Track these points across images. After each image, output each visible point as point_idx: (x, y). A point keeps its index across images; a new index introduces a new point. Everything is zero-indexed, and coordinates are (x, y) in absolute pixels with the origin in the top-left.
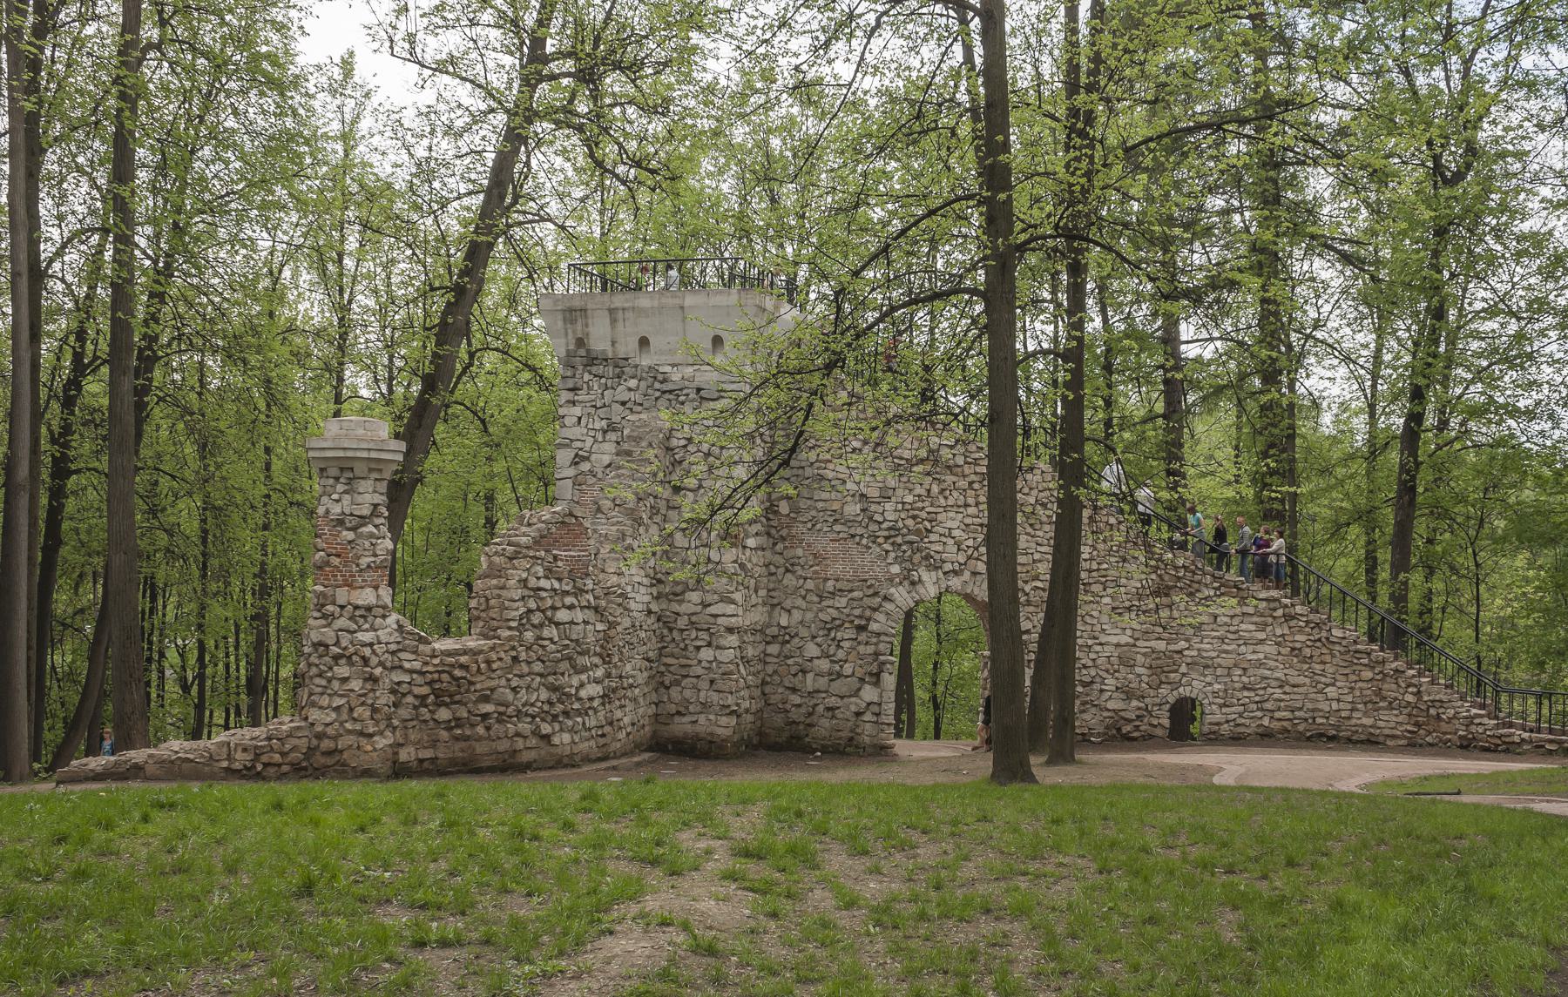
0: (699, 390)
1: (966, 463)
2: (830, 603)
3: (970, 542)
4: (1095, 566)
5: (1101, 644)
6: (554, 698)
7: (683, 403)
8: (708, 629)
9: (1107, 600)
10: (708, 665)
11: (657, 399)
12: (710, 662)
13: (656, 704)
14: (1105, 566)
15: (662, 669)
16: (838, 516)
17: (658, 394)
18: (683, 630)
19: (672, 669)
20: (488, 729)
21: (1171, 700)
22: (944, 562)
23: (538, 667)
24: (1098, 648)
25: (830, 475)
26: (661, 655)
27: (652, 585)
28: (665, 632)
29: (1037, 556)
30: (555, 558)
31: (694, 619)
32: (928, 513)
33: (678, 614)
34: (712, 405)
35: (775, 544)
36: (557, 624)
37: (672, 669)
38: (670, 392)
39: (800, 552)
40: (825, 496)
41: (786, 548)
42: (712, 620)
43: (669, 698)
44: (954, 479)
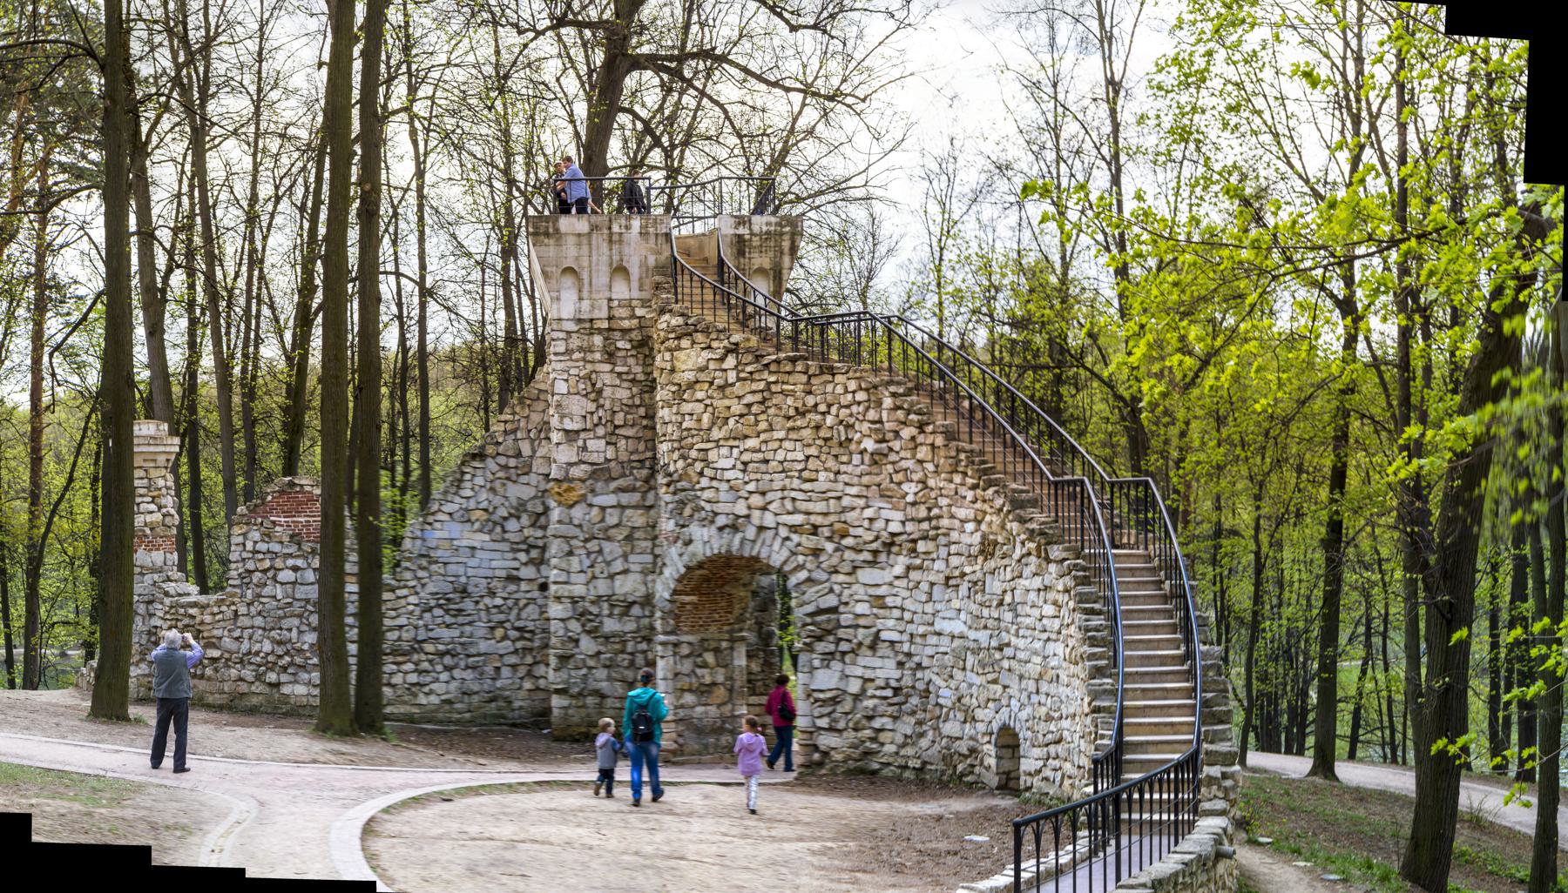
1: (739, 379)
3: (751, 487)
4: (923, 513)
5: (939, 634)
9: (940, 565)
14: (935, 511)
20: (216, 670)
21: (995, 726)
22: (716, 514)
23: (259, 621)
24: (933, 640)
29: (846, 501)
30: (274, 523)
32: (700, 450)
44: (727, 402)
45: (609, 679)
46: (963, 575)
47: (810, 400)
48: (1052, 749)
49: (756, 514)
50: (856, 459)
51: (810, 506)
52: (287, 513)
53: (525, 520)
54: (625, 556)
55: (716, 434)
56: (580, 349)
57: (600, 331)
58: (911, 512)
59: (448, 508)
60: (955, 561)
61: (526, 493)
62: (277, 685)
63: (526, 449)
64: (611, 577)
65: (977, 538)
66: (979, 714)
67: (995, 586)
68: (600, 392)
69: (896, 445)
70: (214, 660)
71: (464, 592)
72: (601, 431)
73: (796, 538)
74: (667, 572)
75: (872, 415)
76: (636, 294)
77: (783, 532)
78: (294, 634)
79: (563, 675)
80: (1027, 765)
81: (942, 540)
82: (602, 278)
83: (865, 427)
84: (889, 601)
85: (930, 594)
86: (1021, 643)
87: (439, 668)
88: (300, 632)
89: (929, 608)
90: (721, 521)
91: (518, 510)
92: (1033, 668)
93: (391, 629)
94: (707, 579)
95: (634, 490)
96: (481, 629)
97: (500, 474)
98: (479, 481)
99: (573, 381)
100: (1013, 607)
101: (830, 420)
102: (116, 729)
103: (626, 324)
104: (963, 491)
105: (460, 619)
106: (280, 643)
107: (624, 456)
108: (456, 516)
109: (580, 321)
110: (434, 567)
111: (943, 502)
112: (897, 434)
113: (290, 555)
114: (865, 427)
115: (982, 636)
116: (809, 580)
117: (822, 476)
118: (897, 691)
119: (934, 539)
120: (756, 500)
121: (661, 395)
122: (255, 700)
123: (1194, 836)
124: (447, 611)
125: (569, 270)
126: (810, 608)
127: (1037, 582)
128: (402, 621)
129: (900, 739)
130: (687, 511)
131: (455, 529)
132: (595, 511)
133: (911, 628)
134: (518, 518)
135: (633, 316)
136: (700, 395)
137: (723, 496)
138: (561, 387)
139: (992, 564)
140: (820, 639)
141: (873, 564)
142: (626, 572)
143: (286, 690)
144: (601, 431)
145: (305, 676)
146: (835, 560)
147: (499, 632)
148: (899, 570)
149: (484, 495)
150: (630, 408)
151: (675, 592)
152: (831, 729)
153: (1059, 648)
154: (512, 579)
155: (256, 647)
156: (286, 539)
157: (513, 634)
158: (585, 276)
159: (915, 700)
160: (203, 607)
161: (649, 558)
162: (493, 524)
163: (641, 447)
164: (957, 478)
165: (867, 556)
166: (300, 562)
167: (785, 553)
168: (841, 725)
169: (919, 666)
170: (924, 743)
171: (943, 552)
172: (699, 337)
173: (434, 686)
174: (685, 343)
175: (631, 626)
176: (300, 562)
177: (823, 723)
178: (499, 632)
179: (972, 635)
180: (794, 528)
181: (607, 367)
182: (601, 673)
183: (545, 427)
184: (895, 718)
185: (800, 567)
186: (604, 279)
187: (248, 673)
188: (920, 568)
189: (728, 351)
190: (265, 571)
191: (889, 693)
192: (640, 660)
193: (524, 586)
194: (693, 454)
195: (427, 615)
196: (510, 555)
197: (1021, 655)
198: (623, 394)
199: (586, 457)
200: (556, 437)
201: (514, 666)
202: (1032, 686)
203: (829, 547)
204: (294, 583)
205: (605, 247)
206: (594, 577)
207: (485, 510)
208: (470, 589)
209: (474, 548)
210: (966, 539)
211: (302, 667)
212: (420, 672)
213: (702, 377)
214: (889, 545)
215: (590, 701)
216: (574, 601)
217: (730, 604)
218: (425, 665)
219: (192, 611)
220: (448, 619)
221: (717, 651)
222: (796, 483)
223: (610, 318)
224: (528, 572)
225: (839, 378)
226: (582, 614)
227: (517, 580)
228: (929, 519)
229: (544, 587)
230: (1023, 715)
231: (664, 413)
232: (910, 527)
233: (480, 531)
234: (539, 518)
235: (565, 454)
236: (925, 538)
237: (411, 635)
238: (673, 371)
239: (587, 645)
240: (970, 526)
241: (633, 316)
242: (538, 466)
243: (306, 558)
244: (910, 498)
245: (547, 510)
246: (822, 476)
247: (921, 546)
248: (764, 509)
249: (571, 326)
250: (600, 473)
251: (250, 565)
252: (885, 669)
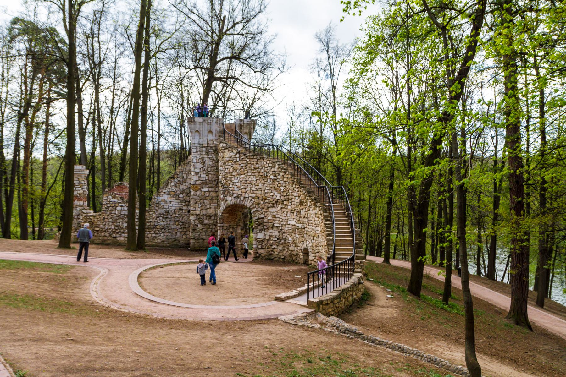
3: (243, 187)
4: (285, 194)
6: (116, 228)
21: (303, 248)
23: (111, 220)
24: (287, 226)
27: (181, 202)
29: (266, 191)
45: (206, 235)
46: (295, 210)
47: (258, 166)
48: (317, 254)
49: (244, 194)
50: (269, 180)
51: (257, 192)
52: (120, 191)
53: (184, 194)
54: (210, 204)
55: (234, 174)
56: (200, 151)
57: (205, 147)
58: (282, 194)
59: (164, 191)
60: (293, 206)
61: (185, 187)
62: (115, 237)
63: (185, 176)
64: (207, 209)
65: (299, 201)
66: (299, 245)
67: (303, 213)
68: (204, 162)
69: (279, 177)
70: (97, 231)
71: (168, 213)
72: (204, 172)
73: (253, 200)
74: (221, 208)
75: (273, 169)
76: (214, 138)
77: (250, 198)
78: (121, 224)
79: (194, 234)
80: (310, 258)
81: (290, 201)
82: (206, 132)
83: (271, 173)
84: (277, 216)
85: (287, 215)
86: (309, 227)
88: (123, 223)
89: (286, 218)
90: (235, 195)
91: (183, 192)
92: (312, 234)
93: (148, 222)
94: (231, 210)
95: (213, 187)
96: (172, 222)
98: (173, 184)
99: (198, 159)
100: (307, 218)
101: (262, 171)
102: (66, 251)
103: (211, 145)
104: (295, 189)
106: (117, 226)
107: (210, 179)
109: (200, 144)
111: (290, 191)
112: (279, 174)
113: (120, 203)
114: (271, 173)
115: (300, 225)
116: (257, 211)
117: (260, 185)
118: (278, 239)
119: (288, 201)
120: (244, 190)
121: (220, 163)
122: (109, 242)
123: (353, 278)
124: (163, 218)
125: (197, 131)
126: (256, 218)
127: (314, 212)
128: (151, 220)
129: (279, 251)
130: (226, 193)
131: (165, 197)
132: (203, 193)
133: (282, 223)
135: (213, 143)
136: (230, 164)
137: (235, 189)
138: (195, 161)
139: (302, 207)
140: (259, 225)
141: (273, 207)
142: (210, 208)
143: (118, 239)
144: (204, 172)
145: (123, 235)
146: (263, 206)
147: (177, 223)
148: (279, 208)
149: (173, 188)
150: (212, 167)
151: (223, 213)
152: (261, 248)
153: (319, 229)
154: (181, 209)
155: (110, 227)
157: (181, 223)
158: (201, 132)
159: (283, 241)
160: (94, 216)
161: (216, 205)
162: (176, 195)
163: (215, 176)
164: (294, 186)
165: (271, 205)
166: (123, 205)
167: (251, 204)
168: (264, 247)
169: (284, 233)
170: (285, 252)
171: (290, 204)
172: (230, 149)
173: (160, 237)
174: (226, 151)
175: (211, 222)
176: (123, 205)
177: (260, 247)
178: (177, 223)
179: (297, 225)
180: (253, 198)
181: (206, 156)
182: (203, 234)
183: (190, 171)
184: (278, 246)
185: (254, 207)
186: (206, 134)
187: (107, 234)
188: (284, 208)
189: (237, 153)
190: (113, 207)
191: (276, 239)
192: (213, 231)
194: (228, 179)
197: (309, 230)
198: (210, 163)
199: (201, 179)
200: (193, 173)
201: (181, 232)
202: (312, 238)
203: (262, 202)
204: (121, 210)
205: (206, 125)
206: (202, 209)
209: (171, 202)
210: (296, 201)
211: (123, 233)
213: (231, 159)
214: (277, 202)
215: (201, 241)
216: (197, 215)
217: (237, 217)
218: (157, 232)
219: (91, 218)
220: (163, 220)
221: (233, 228)
222: (254, 186)
223: (208, 144)
224: (185, 208)
225: (265, 160)
226: (199, 218)
227: (182, 210)
228: (287, 196)
229: (189, 212)
230: (310, 245)
231: (221, 168)
232: (282, 198)
233: (173, 197)
234: (188, 194)
235: (195, 178)
236: (286, 200)
238: (223, 157)
239: (199, 226)
240: (297, 198)
241: (213, 143)
242: (188, 181)
244: (282, 191)
245: (190, 192)
246: (260, 185)
247: (285, 203)
248: (246, 192)
249: (198, 145)
250: (204, 183)
251: (109, 205)
252: (275, 233)
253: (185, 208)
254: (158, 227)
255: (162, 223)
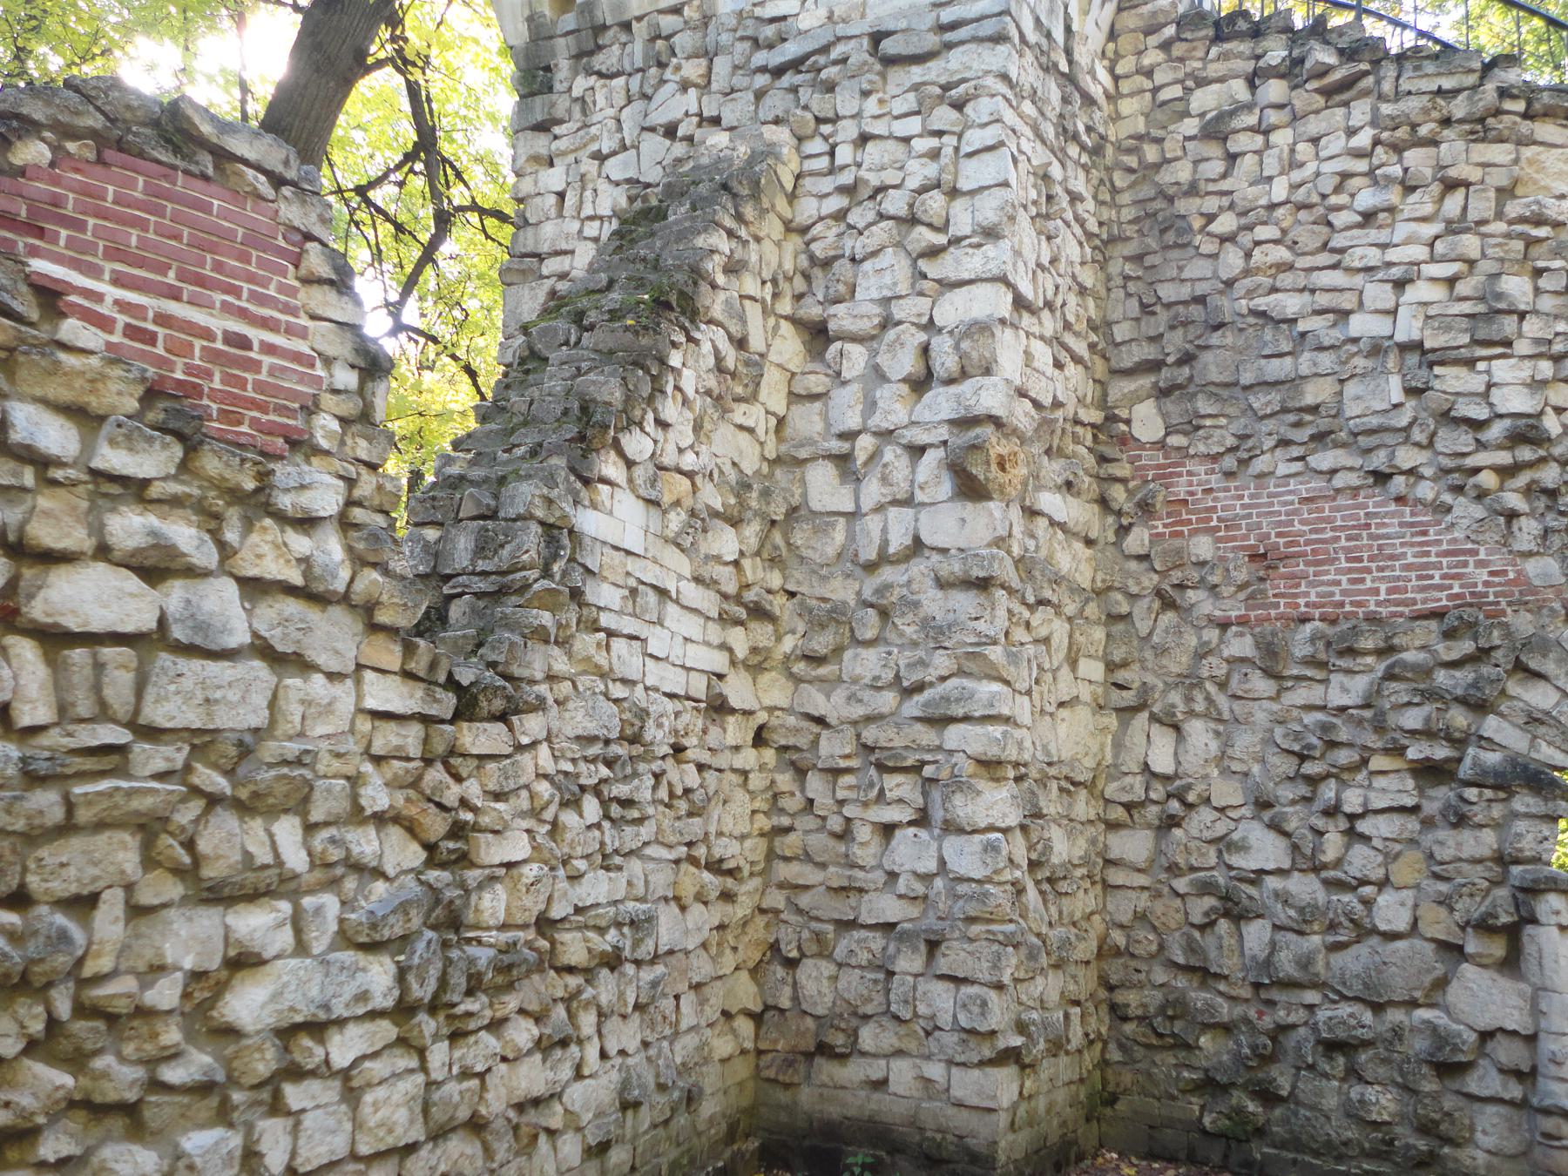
0: (877, 38)
2: (1313, 694)
7: (830, 87)
8: (917, 768)
10: (920, 889)
11: (760, 95)
12: (926, 878)
13: (757, 1018)
15: (776, 899)
16: (1323, 424)
17: (762, 80)
18: (837, 772)
19: (804, 900)
25: (1291, 304)
26: (771, 855)
27: (725, 620)
28: (785, 780)
30: (50, 297)
31: (870, 734)
33: (820, 721)
34: (916, 73)
35: (1123, 531)
36: (54, 639)
37: (804, 900)
38: (795, 65)
39: (1203, 547)
40: (1277, 369)
41: (1156, 538)
42: (926, 736)
43: (795, 999)
53: (752, 530)
87: (588, 1021)
88: (137, 912)
97: (712, 382)
105: (630, 837)
108: (640, 473)
110: (586, 643)
113: (136, 490)
128: (516, 847)
134: (735, 523)
156: (121, 397)
166: (184, 535)
173: (576, 1095)
176: (184, 535)
193: (735, 731)
195: (569, 818)
196: (715, 633)
207: (689, 475)
208: (651, 732)
209: (662, 593)
212: (544, 1046)
237: (533, 905)
243: (212, 522)
253: (738, 691)
254: (574, 948)
255: (597, 888)
